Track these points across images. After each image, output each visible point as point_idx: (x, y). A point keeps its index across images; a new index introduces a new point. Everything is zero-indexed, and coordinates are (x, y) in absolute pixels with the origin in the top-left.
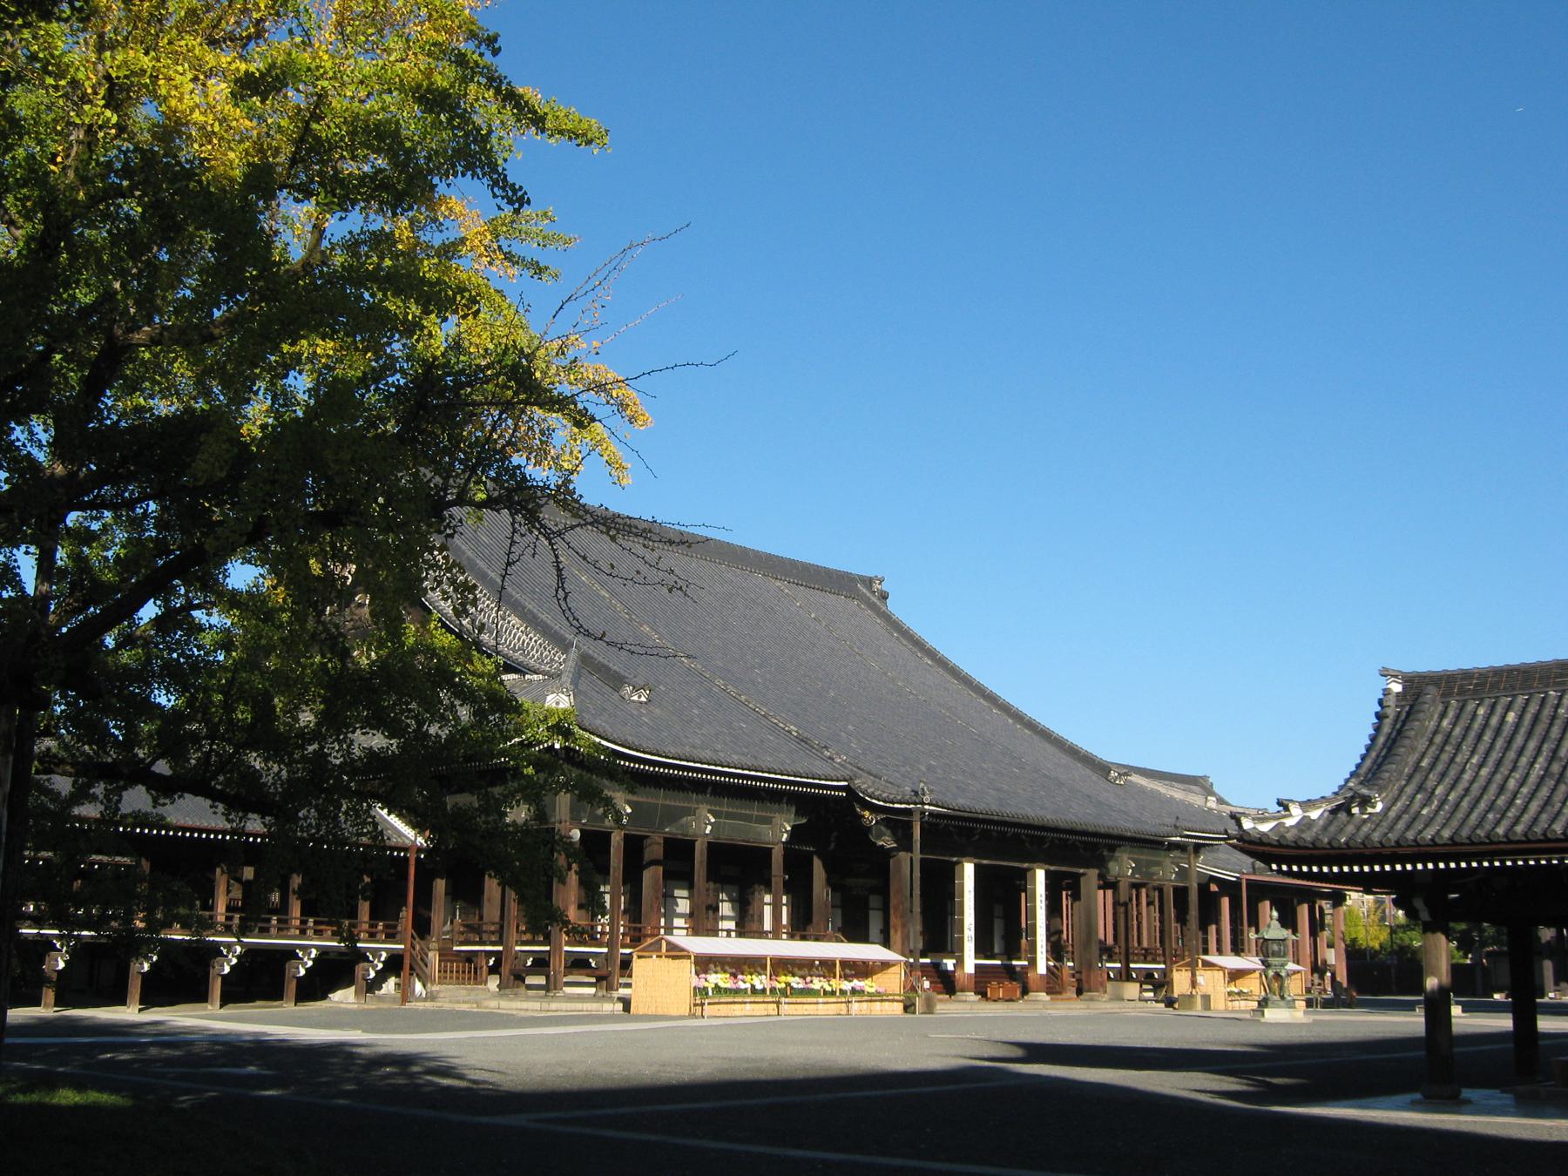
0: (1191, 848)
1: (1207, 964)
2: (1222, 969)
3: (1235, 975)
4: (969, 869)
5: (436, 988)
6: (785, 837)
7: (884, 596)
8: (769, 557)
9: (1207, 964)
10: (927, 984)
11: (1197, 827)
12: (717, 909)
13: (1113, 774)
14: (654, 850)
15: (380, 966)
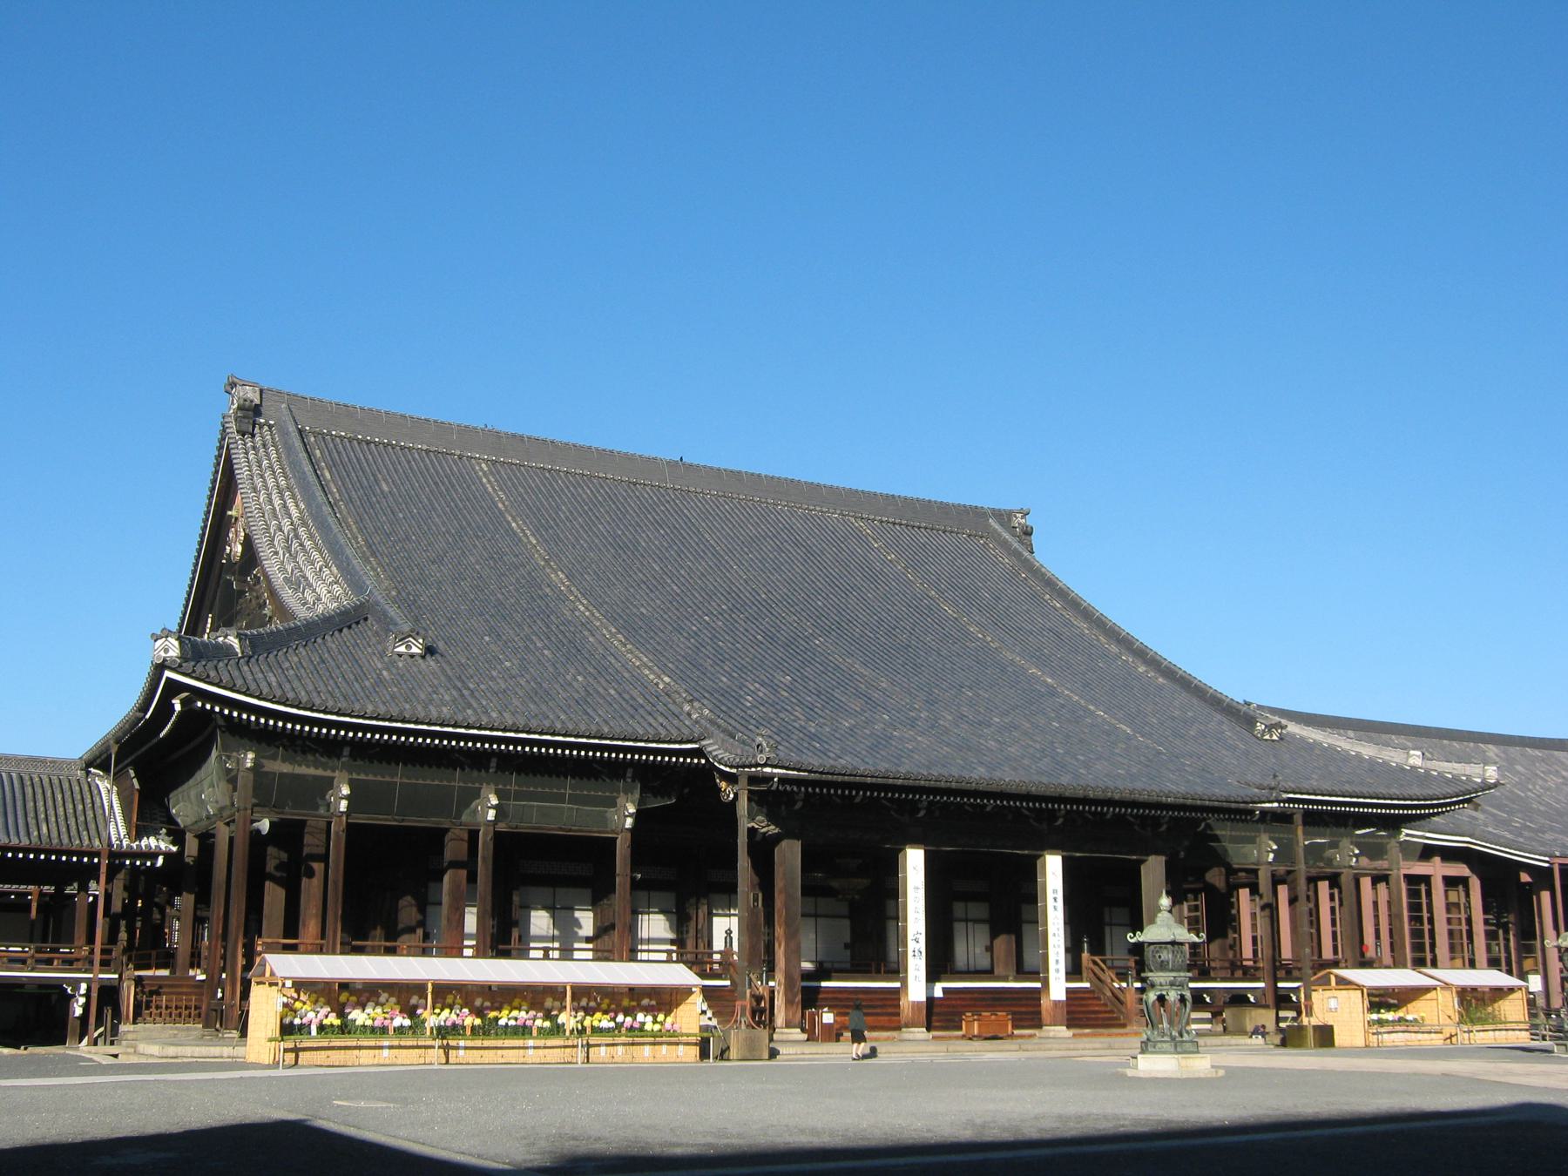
0: (1298, 818)
1: (1343, 983)
2: (1359, 987)
3: (1381, 1000)
4: (914, 861)
5: (131, 1027)
6: (629, 822)
7: (1028, 532)
8: (854, 493)
9: (1343, 983)
10: (828, 1018)
11: (1365, 790)
12: (633, 928)
13: (1260, 727)
14: (454, 848)
15: (82, 1000)
